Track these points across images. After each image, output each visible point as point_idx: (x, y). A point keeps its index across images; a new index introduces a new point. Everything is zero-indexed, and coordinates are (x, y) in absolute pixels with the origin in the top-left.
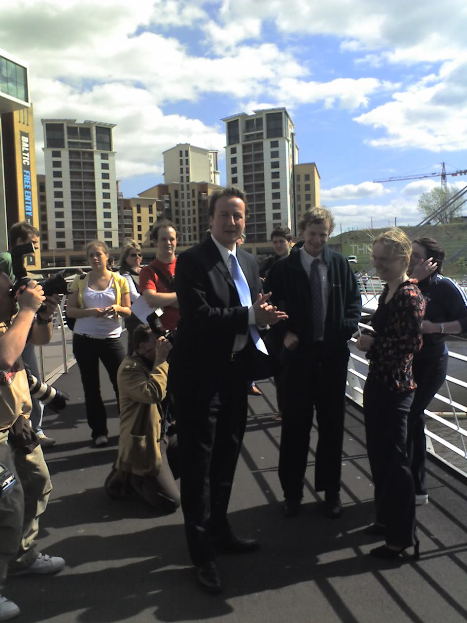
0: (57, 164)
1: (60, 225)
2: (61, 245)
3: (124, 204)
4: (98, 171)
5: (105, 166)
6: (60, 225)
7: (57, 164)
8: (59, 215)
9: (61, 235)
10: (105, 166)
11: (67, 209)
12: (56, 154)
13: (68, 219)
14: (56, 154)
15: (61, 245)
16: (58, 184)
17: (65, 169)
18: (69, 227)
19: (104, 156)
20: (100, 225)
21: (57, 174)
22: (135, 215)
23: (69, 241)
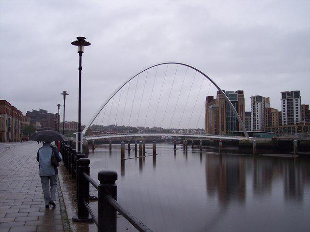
1: (285, 119)
2: (285, 125)
4: (294, 104)
5: (297, 102)
6: (285, 119)
7: (284, 103)
8: (284, 117)
10: (297, 102)
11: (286, 115)
12: (284, 101)
13: (286, 118)
14: (284, 101)
15: (285, 125)
17: (286, 104)
18: (286, 119)
19: (297, 100)
20: (295, 119)
21: (284, 106)
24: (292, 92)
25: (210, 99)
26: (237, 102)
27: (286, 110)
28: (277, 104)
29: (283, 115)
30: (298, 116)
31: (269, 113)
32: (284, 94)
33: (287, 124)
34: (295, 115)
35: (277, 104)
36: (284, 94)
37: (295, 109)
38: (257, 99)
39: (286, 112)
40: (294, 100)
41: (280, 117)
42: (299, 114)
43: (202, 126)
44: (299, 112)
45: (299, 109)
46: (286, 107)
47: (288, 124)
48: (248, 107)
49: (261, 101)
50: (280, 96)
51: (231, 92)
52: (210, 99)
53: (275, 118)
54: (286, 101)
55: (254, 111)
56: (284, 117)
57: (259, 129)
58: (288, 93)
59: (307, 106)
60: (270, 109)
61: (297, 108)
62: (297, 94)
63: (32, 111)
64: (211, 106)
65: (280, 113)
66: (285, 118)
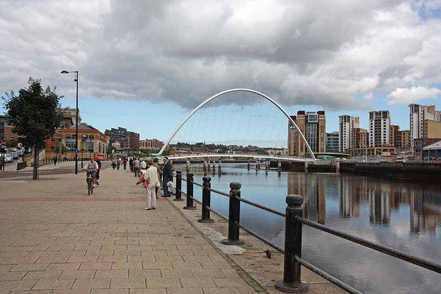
4: (382, 125)
5: (385, 123)
13: (373, 139)
17: (373, 125)
26: (318, 124)
27: (374, 131)
28: (365, 125)
29: (370, 137)
30: (386, 138)
31: (357, 133)
32: (371, 114)
35: (365, 125)
38: (345, 119)
39: (374, 133)
40: (382, 120)
42: (387, 136)
44: (387, 133)
46: (373, 128)
47: (376, 146)
48: (332, 126)
49: (349, 121)
51: (312, 113)
53: (364, 138)
55: (342, 132)
58: (377, 113)
59: (397, 127)
60: (358, 129)
62: (385, 114)
63: (110, 129)
66: (372, 139)
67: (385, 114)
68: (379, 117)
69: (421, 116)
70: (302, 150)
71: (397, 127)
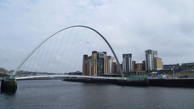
0: (124, 60)
2: (124, 71)
3: (135, 65)
4: (129, 60)
5: (130, 60)
7: (124, 60)
8: (124, 67)
9: (124, 69)
12: (124, 59)
13: (125, 67)
14: (124, 59)
15: (124, 71)
16: (124, 63)
19: (131, 58)
20: (130, 68)
21: (124, 61)
22: (138, 66)
23: (125, 70)
24: (128, 55)
25: (86, 57)
28: (121, 60)
32: (124, 55)
33: (125, 71)
34: (130, 66)
35: (121, 60)
36: (124, 55)
37: (129, 63)
40: (129, 59)
41: (122, 67)
43: (81, 70)
44: (132, 65)
45: (132, 63)
46: (125, 62)
49: (111, 58)
50: (122, 55)
52: (86, 57)
53: (118, 68)
54: (125, 58)
56: (124, 67)
57: (110, 72)
58: (126, 55)
59: (135, 62)
61: (131, 62)
62: (130, 55)
64: (89, 60)
65: (122, 65)
66: (124, 67)
67: (130, 55)
68: (127, 57)
69: (153, 56)
70: (96, 73)
71: (135, 62)
